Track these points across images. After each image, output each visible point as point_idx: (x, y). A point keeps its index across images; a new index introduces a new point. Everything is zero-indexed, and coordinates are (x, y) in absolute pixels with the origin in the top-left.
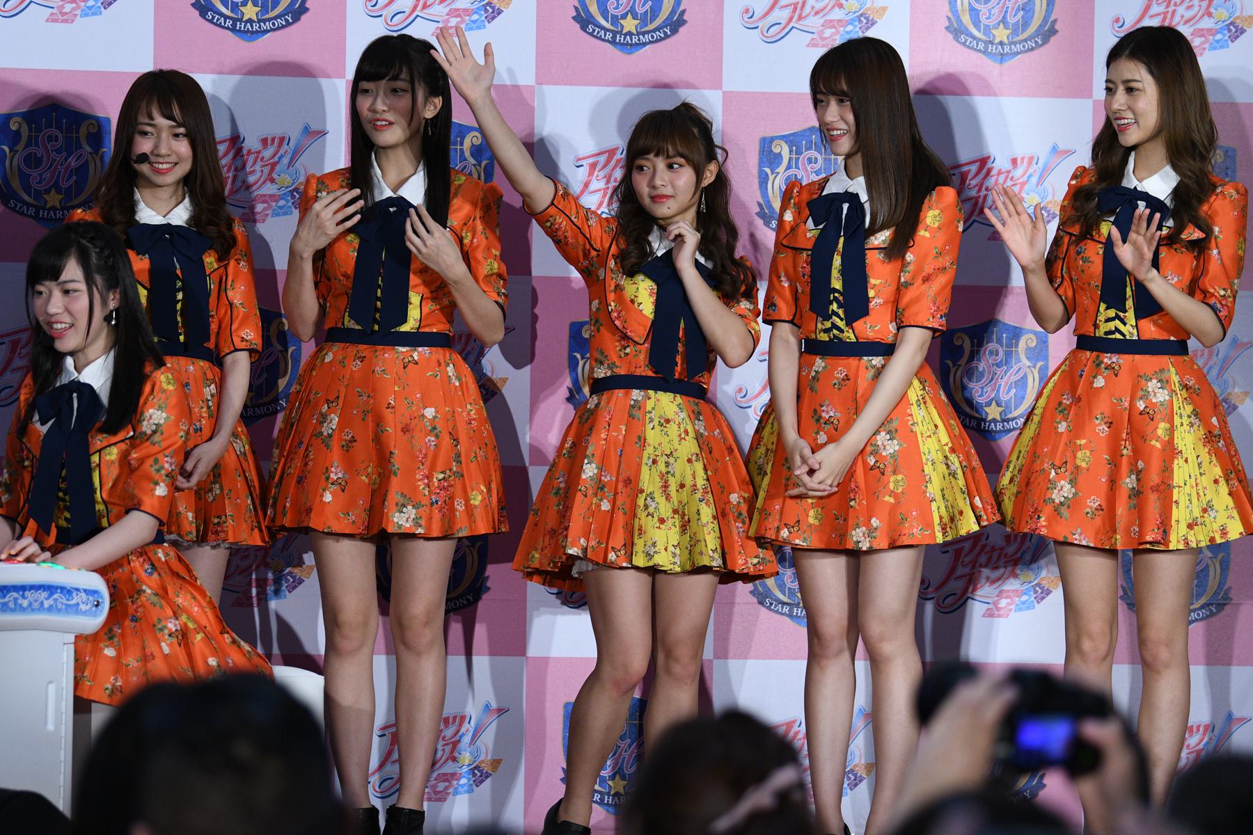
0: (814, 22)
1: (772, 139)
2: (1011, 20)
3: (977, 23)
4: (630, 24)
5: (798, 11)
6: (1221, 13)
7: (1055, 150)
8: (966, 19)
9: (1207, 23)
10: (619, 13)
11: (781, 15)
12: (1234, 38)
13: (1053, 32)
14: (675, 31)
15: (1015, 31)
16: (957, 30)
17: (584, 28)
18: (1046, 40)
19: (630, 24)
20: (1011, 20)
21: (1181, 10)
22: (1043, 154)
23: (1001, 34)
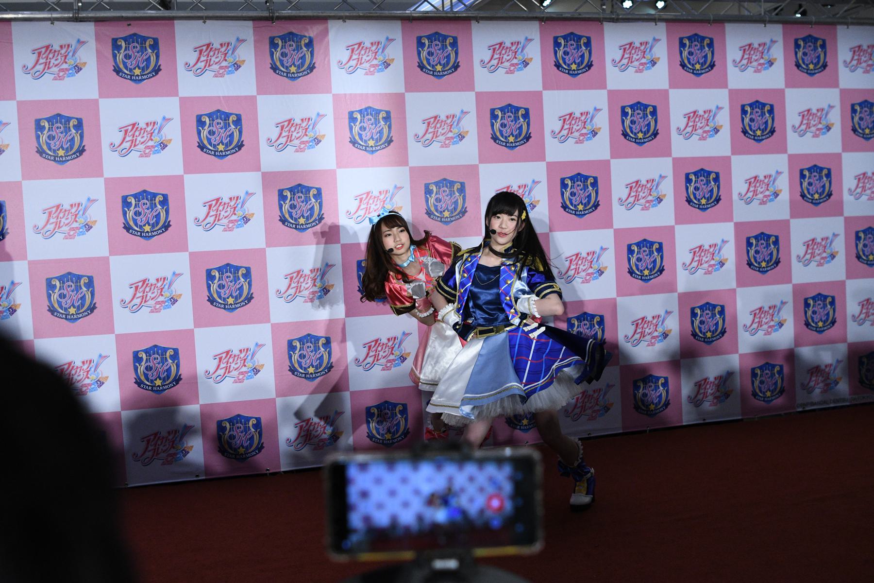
0: (296, 142)
1: (283, 190)
2: (375, 137)
3: (361, 139)
4: (221, 147)
5: (289, 138)
6: (455, 130)
7: (396, 187)
8: (357, 138)
9: (450, 135)
10: (216, 143)
11: (283, 140)
12: (461, 140)
13: (391, 141)
14: (240, 149)
15: (377, 142)
16: (353, 142)
17: (202, 150)
18: (389, 144)
19: (221, 147)
20: (375, 137)
21: (440, 130)
22: (391, 188)
23: (371, 143)
